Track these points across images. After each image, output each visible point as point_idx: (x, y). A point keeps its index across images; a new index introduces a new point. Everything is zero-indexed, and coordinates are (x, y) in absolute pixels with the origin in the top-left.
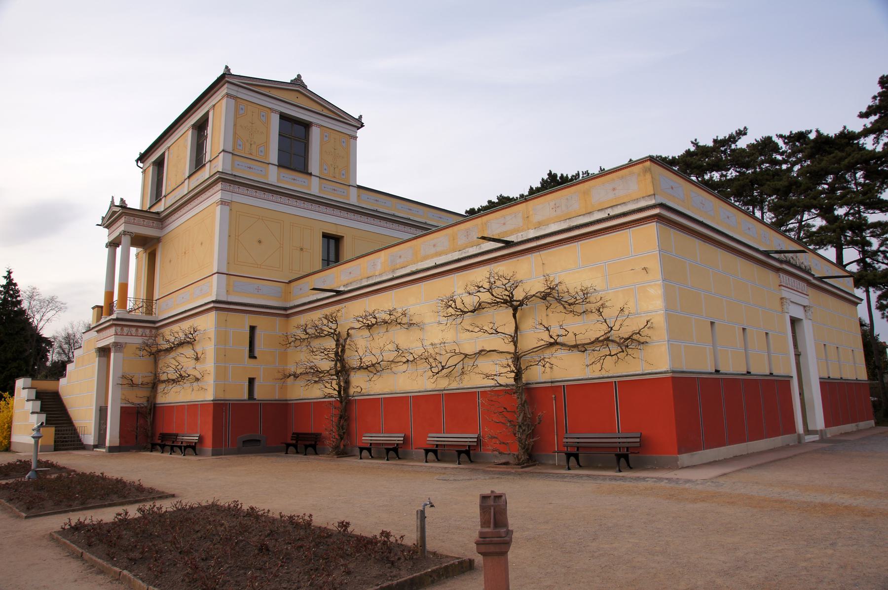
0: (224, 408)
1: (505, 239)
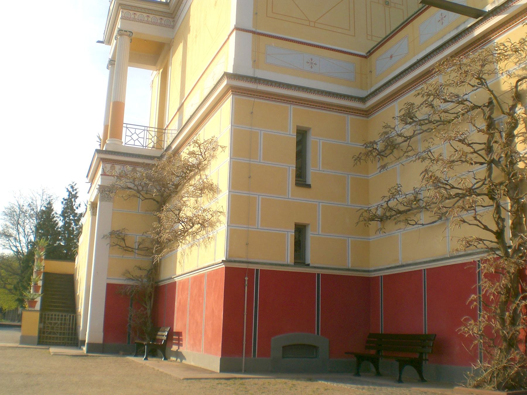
0: (246, 278)
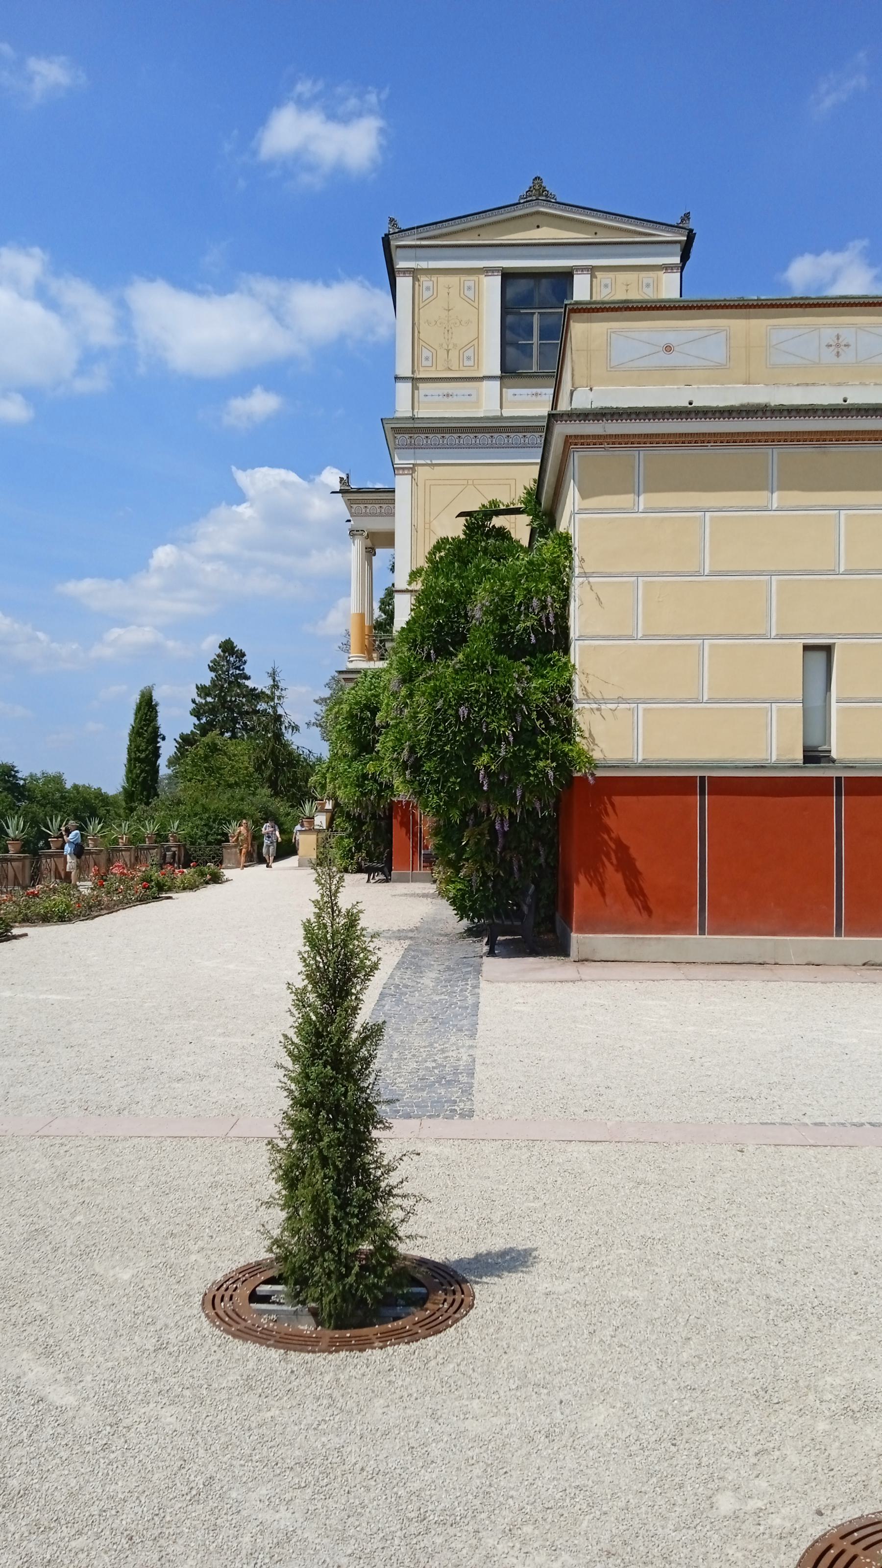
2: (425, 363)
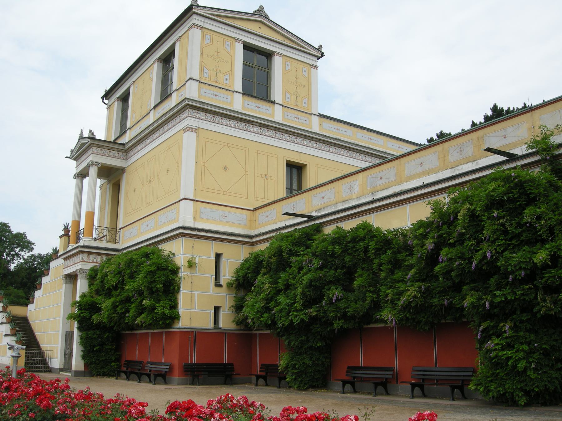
1: (511, 152)
2: (205, 75)
